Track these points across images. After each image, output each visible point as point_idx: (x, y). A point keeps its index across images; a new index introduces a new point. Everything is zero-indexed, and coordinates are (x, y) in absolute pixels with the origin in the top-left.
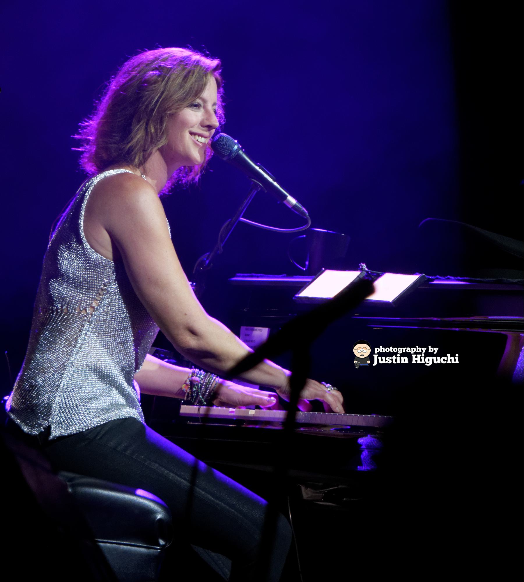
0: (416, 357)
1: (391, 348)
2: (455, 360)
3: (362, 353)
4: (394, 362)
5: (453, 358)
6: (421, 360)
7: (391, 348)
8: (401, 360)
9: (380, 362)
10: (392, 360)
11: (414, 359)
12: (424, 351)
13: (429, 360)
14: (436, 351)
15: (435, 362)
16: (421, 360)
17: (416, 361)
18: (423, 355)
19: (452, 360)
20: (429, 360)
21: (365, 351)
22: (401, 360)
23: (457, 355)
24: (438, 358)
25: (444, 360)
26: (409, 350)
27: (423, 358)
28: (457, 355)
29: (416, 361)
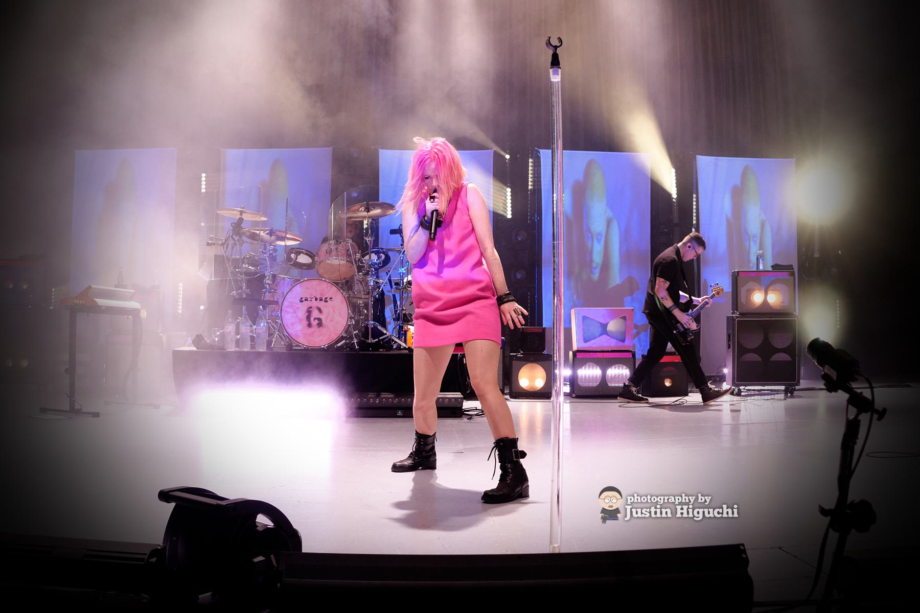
0: (682, 509)
1: (649, 497)
2: (733, 513)
3: (611, 504)
4: (653, 515)
5: (730, 511)
6: (688, 513)
7: (649, 497)
8: (661, 513)
9: (634, 515)
10: (650, 512)
11: (679, 511)
12: (692, 501)
13: (698, 513)
14: (708, 501)
15: (707, 515)
16: (688, 513)
17: (682, 514)
18: (691, 506)
19: (727, 512)
20: (698, 513)
21: (614, 501)
22: (661, 513)
23: (736, 506)
24: (711, 510)
25: (718, 513)
26: (672, 499)
27: (691, 511)
28: (736, 506)
29: (682, 514)
